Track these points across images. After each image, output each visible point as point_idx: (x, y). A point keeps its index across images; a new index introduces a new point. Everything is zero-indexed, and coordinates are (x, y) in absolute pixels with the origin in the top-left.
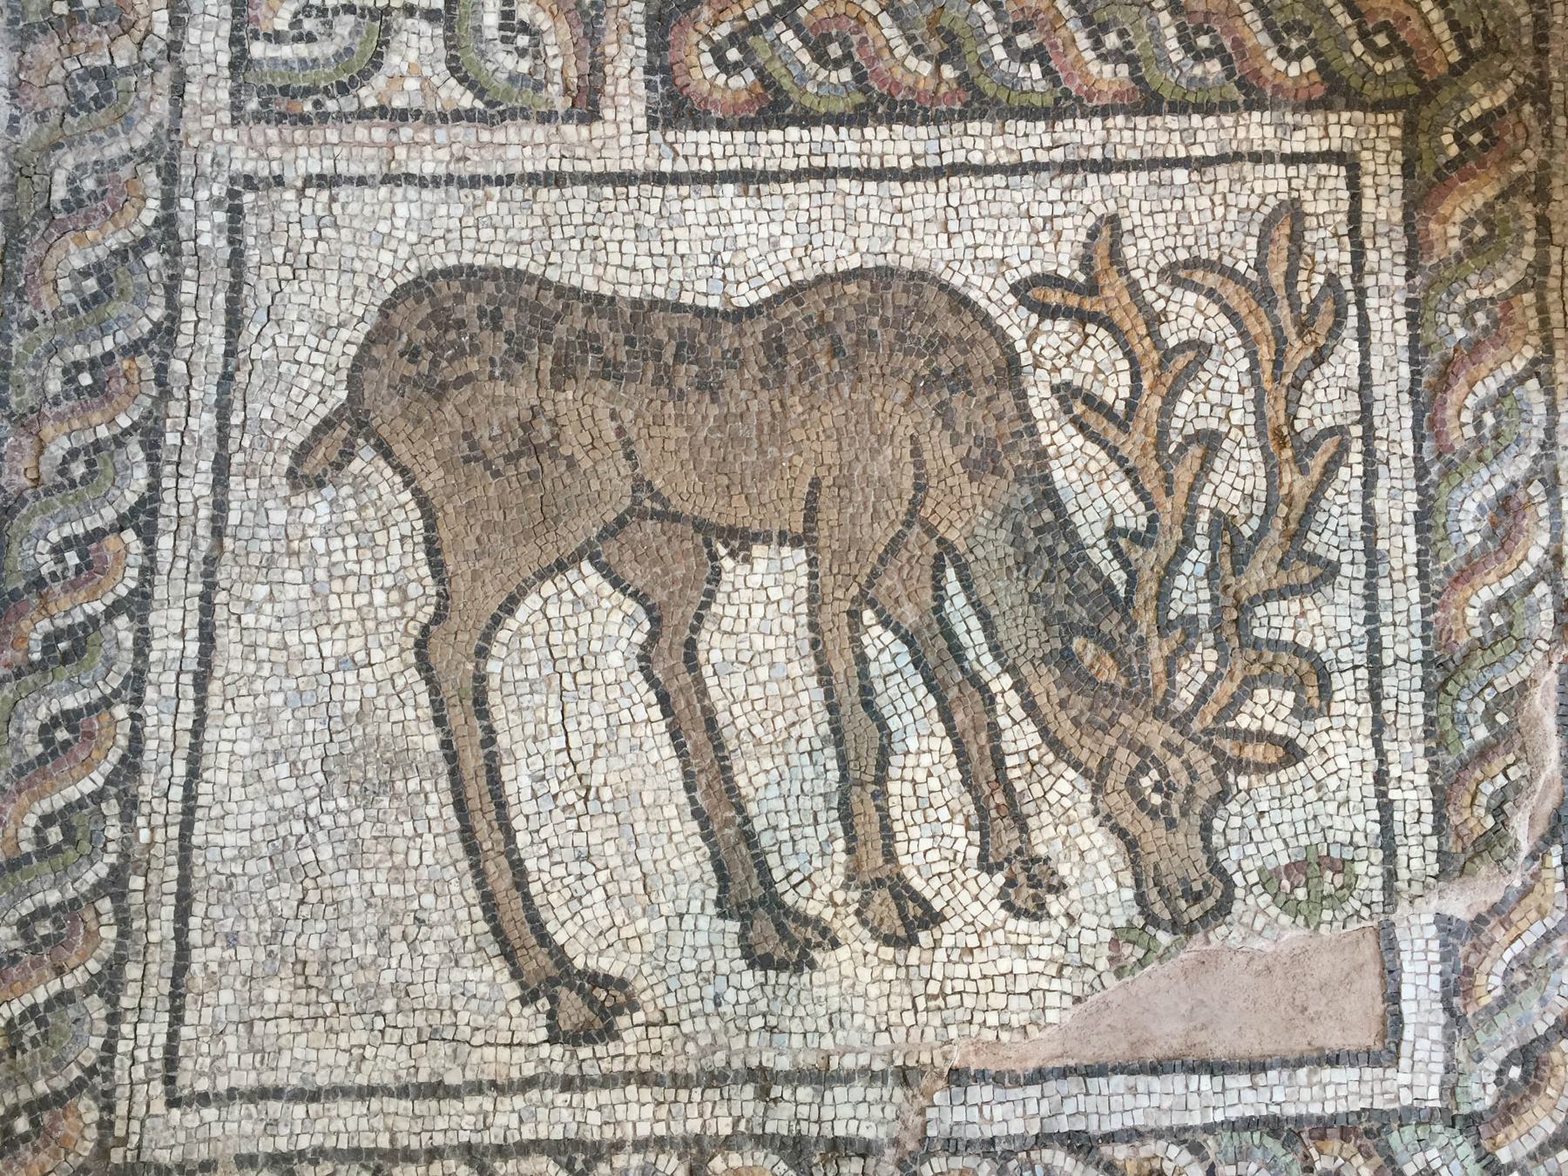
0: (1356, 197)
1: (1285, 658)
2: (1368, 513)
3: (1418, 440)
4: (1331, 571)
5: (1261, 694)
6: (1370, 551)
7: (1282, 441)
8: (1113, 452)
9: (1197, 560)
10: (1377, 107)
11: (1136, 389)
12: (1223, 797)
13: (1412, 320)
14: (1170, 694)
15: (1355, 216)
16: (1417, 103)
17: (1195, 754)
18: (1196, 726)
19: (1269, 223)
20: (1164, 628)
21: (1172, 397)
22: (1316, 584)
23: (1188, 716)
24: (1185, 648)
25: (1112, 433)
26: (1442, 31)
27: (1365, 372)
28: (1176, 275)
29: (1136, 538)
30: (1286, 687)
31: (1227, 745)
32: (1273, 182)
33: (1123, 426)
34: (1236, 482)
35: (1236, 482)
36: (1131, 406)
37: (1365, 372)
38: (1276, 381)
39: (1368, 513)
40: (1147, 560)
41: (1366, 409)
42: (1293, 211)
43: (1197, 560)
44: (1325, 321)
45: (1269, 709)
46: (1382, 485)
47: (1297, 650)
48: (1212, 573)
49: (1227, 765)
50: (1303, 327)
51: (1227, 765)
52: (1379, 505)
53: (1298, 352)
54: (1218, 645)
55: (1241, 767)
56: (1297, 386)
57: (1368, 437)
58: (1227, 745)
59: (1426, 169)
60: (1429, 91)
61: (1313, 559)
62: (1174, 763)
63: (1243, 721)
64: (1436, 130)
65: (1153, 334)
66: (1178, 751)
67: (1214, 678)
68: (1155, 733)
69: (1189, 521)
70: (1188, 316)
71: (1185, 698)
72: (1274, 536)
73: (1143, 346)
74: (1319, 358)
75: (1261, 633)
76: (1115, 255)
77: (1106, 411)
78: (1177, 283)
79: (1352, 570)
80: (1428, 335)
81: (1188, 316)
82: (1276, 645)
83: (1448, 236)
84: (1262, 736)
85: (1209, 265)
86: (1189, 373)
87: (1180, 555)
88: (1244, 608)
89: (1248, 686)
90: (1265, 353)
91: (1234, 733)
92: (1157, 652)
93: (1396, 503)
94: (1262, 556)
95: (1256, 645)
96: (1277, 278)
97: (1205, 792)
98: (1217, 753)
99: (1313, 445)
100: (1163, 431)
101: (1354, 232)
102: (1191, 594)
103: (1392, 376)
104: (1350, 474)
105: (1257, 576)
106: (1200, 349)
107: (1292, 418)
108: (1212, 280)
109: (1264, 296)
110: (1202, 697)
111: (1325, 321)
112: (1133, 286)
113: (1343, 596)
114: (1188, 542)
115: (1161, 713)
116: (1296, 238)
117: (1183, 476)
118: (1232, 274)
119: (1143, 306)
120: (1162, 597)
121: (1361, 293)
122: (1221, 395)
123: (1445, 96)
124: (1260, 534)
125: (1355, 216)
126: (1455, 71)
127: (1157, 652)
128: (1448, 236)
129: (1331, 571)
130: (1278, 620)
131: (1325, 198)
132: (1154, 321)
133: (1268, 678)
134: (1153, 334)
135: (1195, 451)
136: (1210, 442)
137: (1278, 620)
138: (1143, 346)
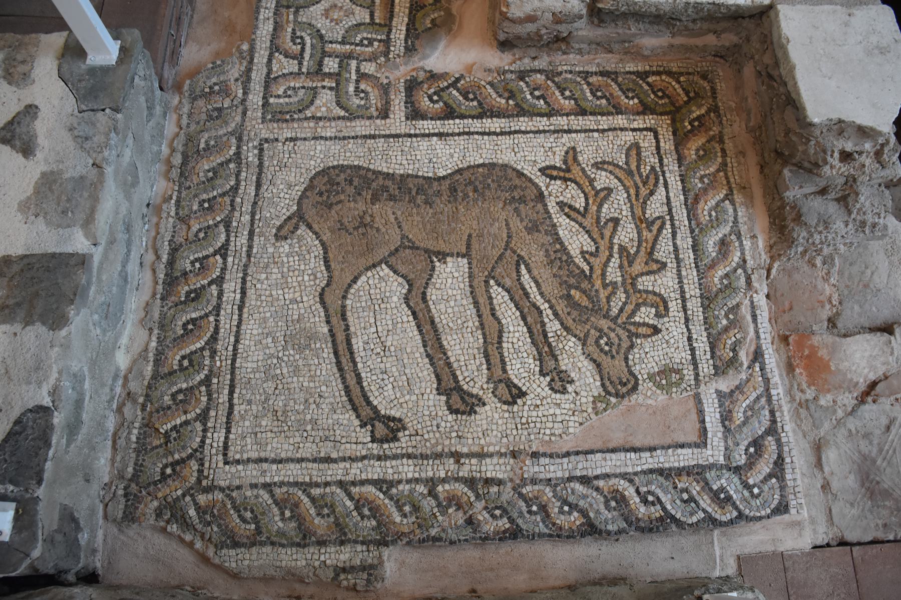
0: (658, 142)
1: (650, 296)
2: (675, 245)
3: (690, 220)
4: (664, 265)
5: (643, 309)
6: (677, 258)
7: (642, 222)
8: (581, 225)
9: (615, 262)
10: (661, 114)
11: (587, 204)
12: (632, 346)
13: (682, 181)
14: (609, 310)
15: (658, 148)
16: (674, 113)
17: (620, 331)
18: (619, 321)
19: (629, 150)
20: (605, 286)
21: (600, 206)
22: (659, 270)
23: (617, 317)
24: (614, 293)
25: (580, 218)
26: (680, 91)
27: (668, 198)
28: (598, 166)
29: (591, 254)
30: (652, 306)
31: (632, 328)
32: (629, 137)
33: (584, 216)
34: (627, 234)
35: (627, 234)
36: (586, 209)
37: (668, 198)
38: (638, 201)
39: (675, 245)
40: (597, 262)
41: (670, 210)
42: (636, 146)
43: (615, 262)
44: (652, 181)
45: (646, 315)
46: (679, 236)
47: (655, 294)
48: (621, 267)
49: (631, 335)
50: (645, 183)
51: (631, 335)
52: (678, 242)
53: (644, 192)
54: (626, 292)
55: (638, 336)
56: (645, 203)
57: (672, 219)
58: (632, 328)
59: (680, 133)
60: (678, 109)
61: (657, 261)
62: (612, 335)
63: (637, 319)
64: (683, 121)
65: (591, 185)
66: (614, 330)
67: (625, 304)
68: (604, 324)
69: (611, 248)
70: (603, 179)
71: (615, 311)
72: (642, 253)
73: (588, 189)
74: (652, 193)
75: (641, 287)
76: (575, 159)
77: (578, 211)
78: (598, 168)
79: (672, 265)
80: (688, 186)
81: (603, 179)
82: (647, 292)
83: (691, 153)
84: (645, 324)
85: (609, 163)
86: (606, 198)
87: (609, 260)
88: (634, 279)
89: (638, 306)
90: (632, 191)
91: (634, 324)
92: (603, 294)
93: (685, 242)
94: (638, 260)
95: (640, 291)
96: (633, 167)
97: (625, 345)
98: (629, 331)
99: (653, 222)
100: (598, 218)
101: (658, 153)
102: (614, 274)
103: (678, 199)
104: (667, 231)
105: (637, 268)
106: (609, 191)
107: (644, 213)
108: (611, 168)
109: (630, 173)
110: (621, 310)
111: (652, 181)
112: (583, 170)
113: (669, 274)
114: (611, 256)
115: (606, 316)
116: (639, 154)
117: (607, 233)
118: (617, 166)
119: (587, 177)
120: (603, 275)
121: (663, 172)
122: (618, 205)
123: (684, 111)
124: (638, 251)
125: (658, 148)
126: (686, 103)
127: (603, 294)
128: (691, 153)
129: (664, 265)
130: (645, 283)
131: (647, 142)
132: (591, 181)
133: (645, 304)
134: (591, 185)
135: (611, 225)
136: (616, 221)
137: (645, 283)
138: (588, 189)
